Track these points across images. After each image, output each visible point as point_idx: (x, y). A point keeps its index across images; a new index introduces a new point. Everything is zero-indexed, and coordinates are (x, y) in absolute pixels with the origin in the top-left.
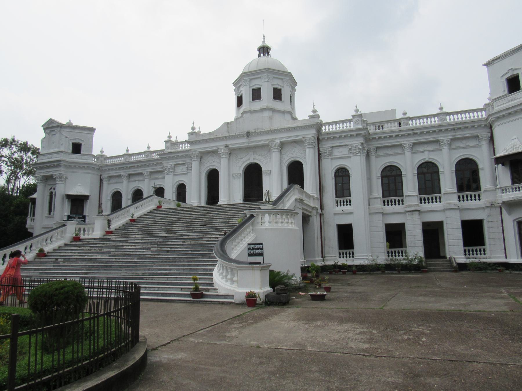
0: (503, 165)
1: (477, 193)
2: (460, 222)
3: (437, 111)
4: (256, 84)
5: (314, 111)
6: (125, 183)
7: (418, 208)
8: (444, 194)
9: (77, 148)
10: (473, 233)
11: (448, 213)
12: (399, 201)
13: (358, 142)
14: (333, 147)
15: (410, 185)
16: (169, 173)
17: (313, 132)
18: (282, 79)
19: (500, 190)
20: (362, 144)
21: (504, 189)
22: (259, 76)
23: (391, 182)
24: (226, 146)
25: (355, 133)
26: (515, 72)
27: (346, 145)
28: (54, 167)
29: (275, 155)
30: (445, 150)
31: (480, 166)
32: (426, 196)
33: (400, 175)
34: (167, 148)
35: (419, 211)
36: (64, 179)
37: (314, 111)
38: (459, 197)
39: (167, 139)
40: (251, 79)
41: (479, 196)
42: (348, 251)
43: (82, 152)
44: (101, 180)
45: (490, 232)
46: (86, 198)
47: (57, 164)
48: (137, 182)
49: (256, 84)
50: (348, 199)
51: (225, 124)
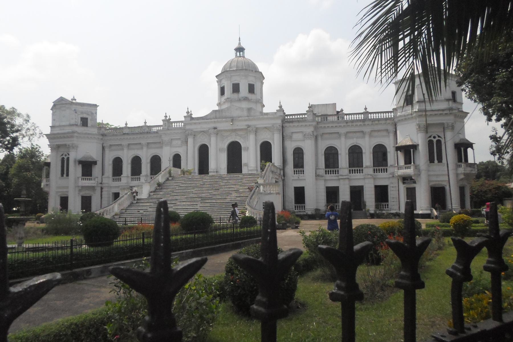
1: (385, 168)
2: (373, 186)
3: (363, 111)
5: (281, 107)
6: (125, 150)
7: (347, 177)
9: (84, 122)
10: (382, 193)
11: (367, 181)
12: (335, 172)
13: (309, 130)
14: (292, 133)
15: (343, 160)
17: (279, 122)
18: (255, 77)
20: (313, 132)
23: (331, 158)
24: (215, 128)
25: (308, 124)
28: (68, 137)
29: (252, 137)
30: (367, 138)
31: (388, 150)
32: (354, 169)
33: (337, 153)
34: (165, 124)
35: (348, 178)
36: (75, 147)
37: (281, 107)
38: (374, 170)
39: (164, 118)
40: (231, 76)
41: (386, 170)
42: (301, 205)
43: (89, 125)
44: (103, 148)
45: (392, 194)
46: (95, 163)
47: (70, 135)
49: (236, 80)
50: (302, 169)
51: (213, 111)
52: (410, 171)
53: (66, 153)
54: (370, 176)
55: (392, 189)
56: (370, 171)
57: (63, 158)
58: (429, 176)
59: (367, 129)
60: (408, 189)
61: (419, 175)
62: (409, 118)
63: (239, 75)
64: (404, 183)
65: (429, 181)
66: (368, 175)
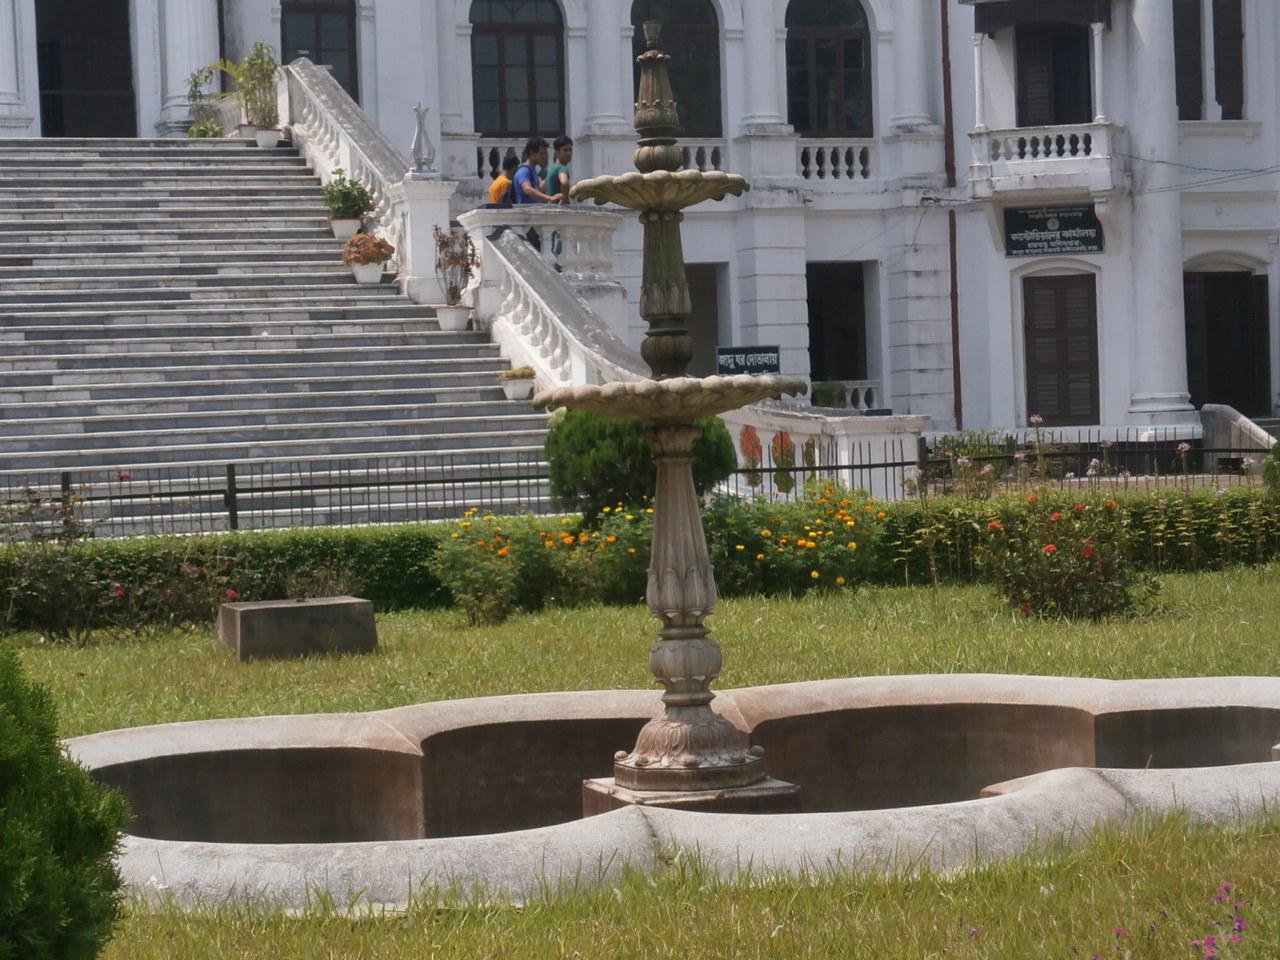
0: (992, 36)
1: (856, 144)
2: (804, 271)
8: (746, 139)
11: (764, 231)
19: (985, 140)
21: (1000, 138)
38: (805, 158)
41: (864, 157)
45: (903, 320)
52: (1085, 170)
54: (784, 200)
55: (913, 285)
56: (779, 160)
58: (1185, 198)
60: (1031, 285)
61: (1129, 190)
64: (1012, 247)
65: (1187, 235)
66: (772, 188)
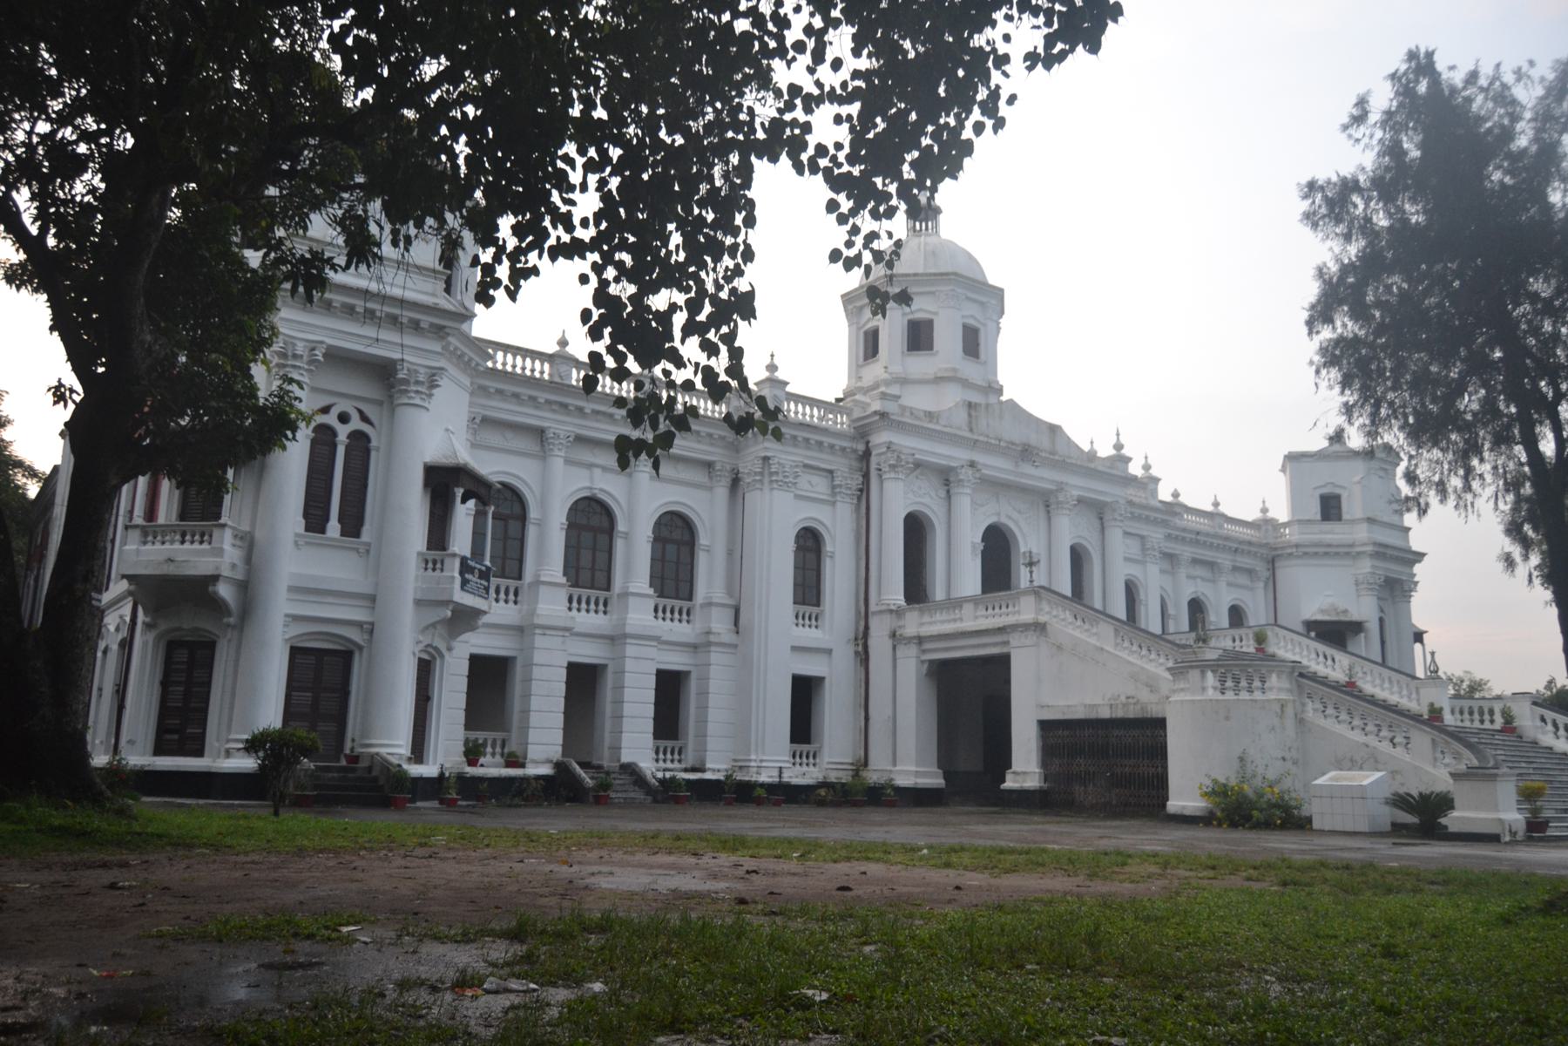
4: (972, 316)
5: (1118, 447)
6: (557, 463)
16: (786, 485)
22: (984, 299)
24: (972, 464)
26: (1337, 491)
27: (1142, 537)
30: (1222, 585)
37: (1118, 447)
48: (597, 472)
49: (971, 313)
53: (343, 406)
57: (334, 433)
59: (1225, 560)
62: (1337, 554)
63: (982, 304)
